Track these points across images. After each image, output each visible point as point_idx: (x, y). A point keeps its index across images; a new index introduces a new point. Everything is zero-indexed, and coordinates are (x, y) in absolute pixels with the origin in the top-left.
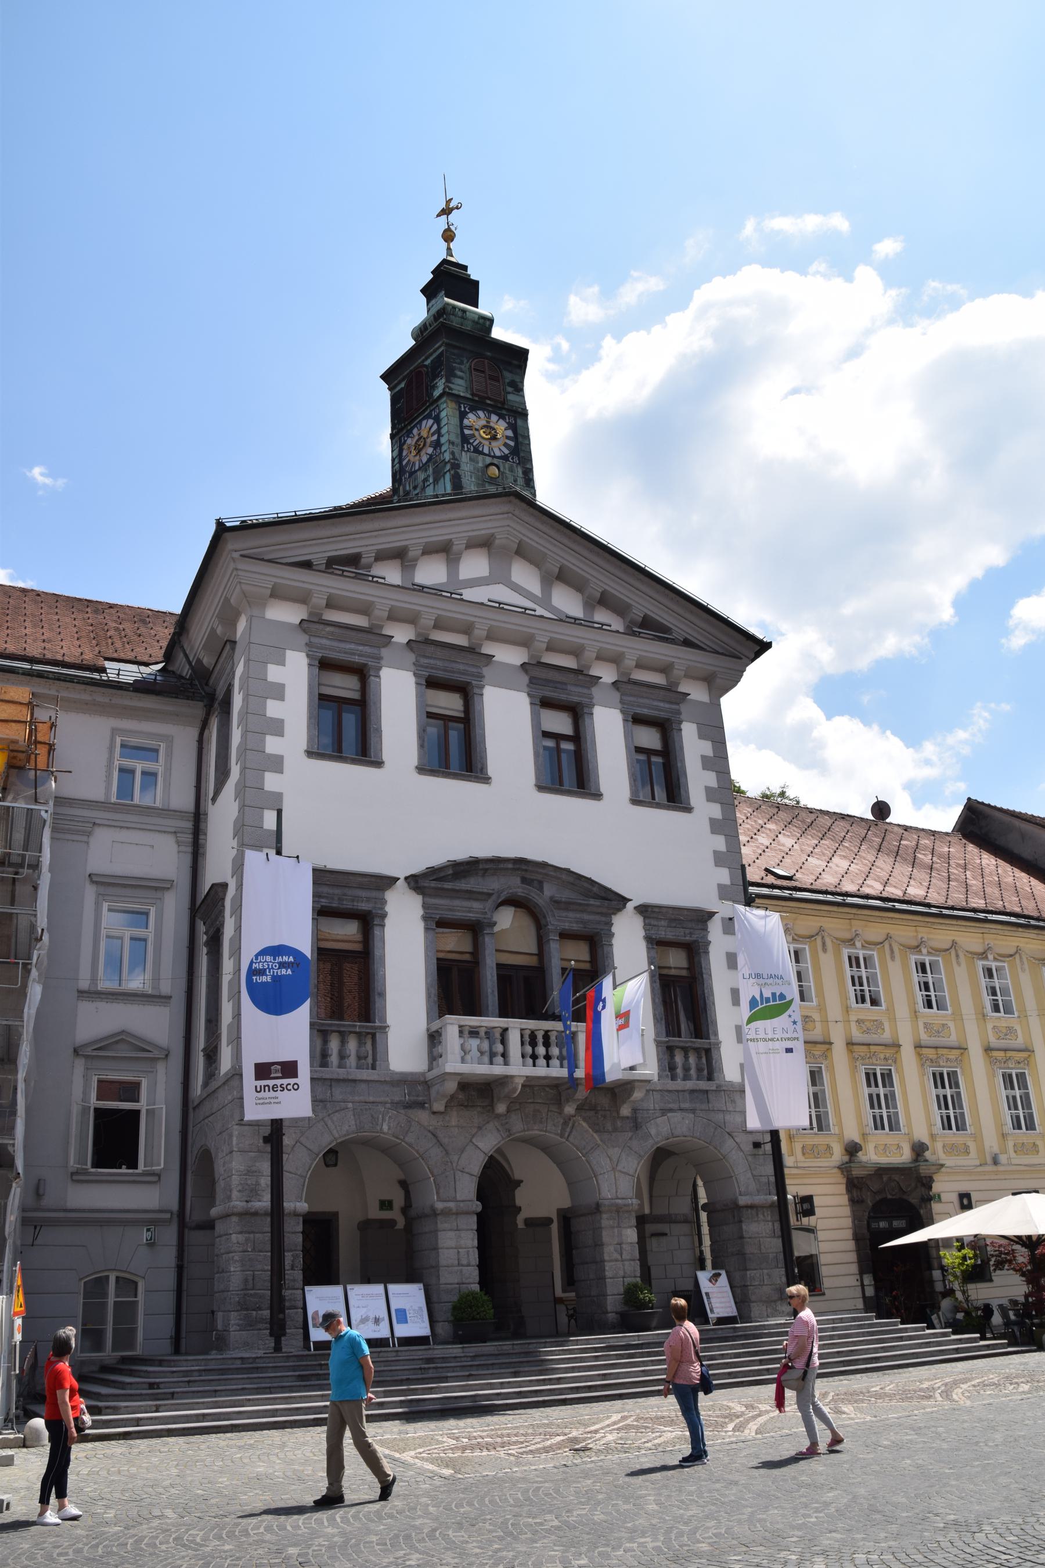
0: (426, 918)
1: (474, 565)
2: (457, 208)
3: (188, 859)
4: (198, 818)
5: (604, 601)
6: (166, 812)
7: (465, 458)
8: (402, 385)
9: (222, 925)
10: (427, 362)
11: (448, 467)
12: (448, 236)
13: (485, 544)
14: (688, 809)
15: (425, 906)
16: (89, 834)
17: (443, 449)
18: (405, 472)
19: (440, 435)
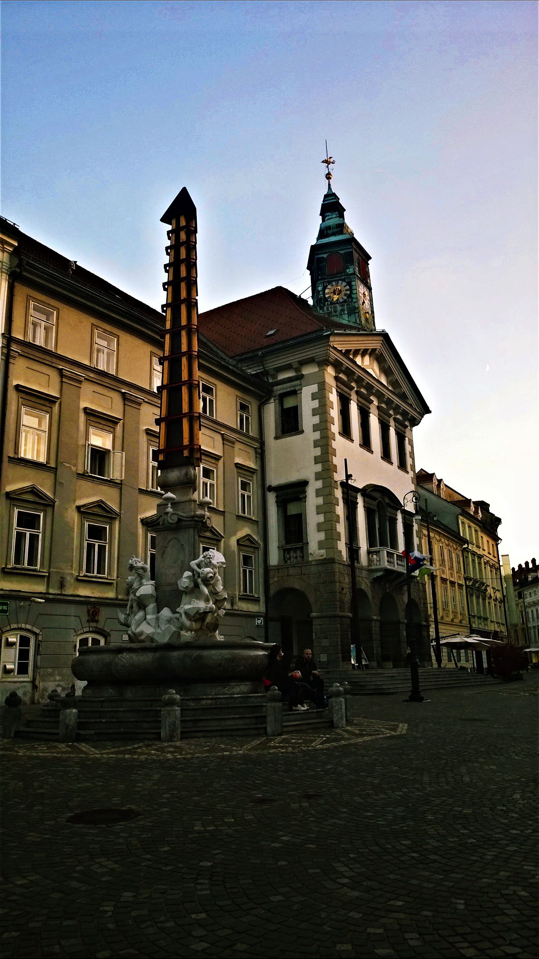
0: (364, 507)
1: (367, 358)
2: (333, 163)
3: (259, 460)
4: (262, 443)
5: (394, 384)
8: (325, 256)
9: (306, 497)
10: (342, 252)
12: (328, 176)
14: (408, 472)
15: (364, 502)
17: (354, 300)
19: (351, 293)
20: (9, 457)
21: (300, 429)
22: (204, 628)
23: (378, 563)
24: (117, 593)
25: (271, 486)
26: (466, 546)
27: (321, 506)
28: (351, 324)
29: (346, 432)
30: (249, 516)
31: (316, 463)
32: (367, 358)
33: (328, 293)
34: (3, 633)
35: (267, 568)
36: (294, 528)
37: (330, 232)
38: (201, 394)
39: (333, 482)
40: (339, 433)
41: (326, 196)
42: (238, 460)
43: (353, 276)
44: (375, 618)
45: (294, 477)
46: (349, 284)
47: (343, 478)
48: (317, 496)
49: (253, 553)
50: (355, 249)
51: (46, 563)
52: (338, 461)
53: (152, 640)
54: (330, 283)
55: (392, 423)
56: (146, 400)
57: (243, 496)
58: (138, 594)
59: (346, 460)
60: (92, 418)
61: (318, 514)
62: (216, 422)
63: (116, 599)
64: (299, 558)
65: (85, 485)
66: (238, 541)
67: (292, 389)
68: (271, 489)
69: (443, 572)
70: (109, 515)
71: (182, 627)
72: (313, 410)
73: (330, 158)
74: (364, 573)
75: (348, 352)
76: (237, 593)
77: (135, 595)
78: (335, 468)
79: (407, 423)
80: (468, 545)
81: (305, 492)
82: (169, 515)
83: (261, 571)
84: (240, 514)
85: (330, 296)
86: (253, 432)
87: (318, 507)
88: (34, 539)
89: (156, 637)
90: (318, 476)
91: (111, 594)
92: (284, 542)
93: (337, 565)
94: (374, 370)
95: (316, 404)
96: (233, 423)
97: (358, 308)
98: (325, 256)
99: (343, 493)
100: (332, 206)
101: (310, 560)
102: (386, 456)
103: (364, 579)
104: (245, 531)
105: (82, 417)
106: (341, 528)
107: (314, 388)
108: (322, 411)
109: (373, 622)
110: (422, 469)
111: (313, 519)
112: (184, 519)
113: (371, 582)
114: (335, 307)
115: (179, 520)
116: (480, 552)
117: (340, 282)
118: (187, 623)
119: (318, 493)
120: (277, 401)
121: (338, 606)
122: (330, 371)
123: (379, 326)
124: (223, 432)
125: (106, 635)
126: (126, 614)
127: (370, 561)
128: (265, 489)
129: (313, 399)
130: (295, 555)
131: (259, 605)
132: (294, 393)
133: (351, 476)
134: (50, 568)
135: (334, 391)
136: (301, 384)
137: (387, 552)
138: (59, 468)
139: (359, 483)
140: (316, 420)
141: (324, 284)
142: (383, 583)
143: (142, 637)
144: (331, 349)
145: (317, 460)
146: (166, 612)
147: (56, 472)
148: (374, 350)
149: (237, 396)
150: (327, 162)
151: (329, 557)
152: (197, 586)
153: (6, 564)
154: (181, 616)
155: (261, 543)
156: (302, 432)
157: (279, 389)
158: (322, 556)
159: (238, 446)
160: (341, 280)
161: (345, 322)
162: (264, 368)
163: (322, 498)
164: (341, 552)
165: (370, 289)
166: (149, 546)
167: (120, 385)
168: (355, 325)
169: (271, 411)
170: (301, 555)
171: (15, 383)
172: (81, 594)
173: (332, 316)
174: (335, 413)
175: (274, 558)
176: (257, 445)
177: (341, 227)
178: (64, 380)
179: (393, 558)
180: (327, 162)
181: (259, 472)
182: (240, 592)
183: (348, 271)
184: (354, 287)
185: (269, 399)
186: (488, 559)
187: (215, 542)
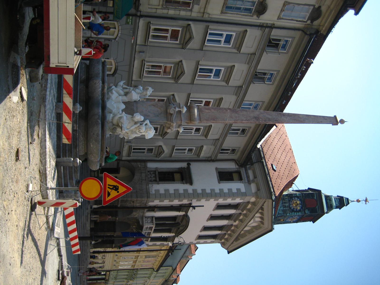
0: (177, 216)
2: (366, 203)
3: (204, 159)
4: (213, 161)
6: (216, 156)
7: (287, 217)
8: (315, 198)
9: (184, 184)
10: (317, 207)
11: (285, 215)
12: (358, 201)
13: (262, 223)
14: (196, 240)
15: (180, 216)
16: (214, 145)
17: (291, 213)
18: (291, 199)
19: (295, 212)
20: (209, 26)
21: (221, 182)
22: (114, 126)
23: (146, 222)
24: (135, 81)
25: (190, 165)
26: (155, 270)
27: (178, 192)
28: (278, 211)
29: (219, 207)
30: (174, 152)
31: (202, 190)
32: (259, 219)
33: (295, 199)
34: (117, 22)
35: (145, 161)
36: (166, 177)
37: (328, 201)
38: (241, 128)
39: (191, 199)
40: (218, 203)
41: (348, 199)
42: (205, 148)
43: (304, 213)
44: (117, 219)
45: (195, 177)
46: (300, 211)
47: (193, 204)
48: (184, 190)
49: (154, 154)
50: (318, 214)
51: (152, 44)
52: (203, 202)
53: (108, 99)
54: (300, 200)
55: (223, 232)
56: (238, 98)
57: (185, 150)
58: (133, 92)
59: (203, 206)
60: (229, 69)
61: (174, 190)
62: (226, 136)
63: (132, 80)
64: (150, 179)
65: (193, 65)
66: (161, 146)
67: (243, 178)
68: (189, 165)
69: (141, 257)
70: (177, 78)
71: (115, 115)
72: (231, 189)
73: (369, 202)
74: (141, 214)
75: (262, 208)
76: (132, 145)
77: (132, 90)
78: (199, 200)
79: (223, 241)
80: (156, 271)
81: (186, 183)
82: (174, 109)
83: (144, 158)
84: (175, 148)
85: (293, 200)
86: (220, 156)
87: (178, 190)
88: (165, 38)
89: (110, 100)
90: (195, 191)
91: (134, 78)
92: (160, 171)
93: (146, 200)
94: (253, 224)
95: (234, 191)
96: (225, 146)
97: (286, 215)
98: (315, 198)
99: (185, 204)
100: (342, 202)
101: (150, 185)
102: (206, 228)
103: (138, 214)
104: (166, 150)
105: (231, 64)
106: (166, 203)
107: (243, 190)
108: (231, 194)
109: (115, 218)
110: (198, 248)
111: (171, 187)
112: (172, 118)
113: (136, 217)
114: (287, 203)
115: (171, 115)
116: (152, 278)
117: (301, 206)
118: (116, 118)
119: (186, 191)
120: (237, 170)
121: (124, 199)
122: (253, 199)
123: (275, 226)
124: (220, 139)
125: (113, 74)
126: (123, 85)
127: (149, 217)
128: (189, 162)
129: (237, 189)
130: (152, 177)
131: (126, 157)
132: (240, 179)
133: (194, 209)
134: (150, 46)
135: (241, 201)
136: (245, 183)
137: (152, 227)
138: (203, 51)
139: (191, 213)
140: (226, 191)
141: (300, 197)
142: (136, 224)
143: (110, 93)
144: (264, 200)
145: (203, 190)
146: (123, 106)
147: (200, 50)
148: (262, 223)
149: (240, 147)
150: (366, 200)
151: (150, 195)
152: (136, 123)
153: (152, 24)
154: (120, 114)
155: (159, 159)
156: (219, 183)
157: (243, 171)
158: (151, 191)
159: (213, 148)
160: (302, 206)
161: (279, 208)
162: (255, 163)
163: (183, 192)
164: (153, 202)
165: (297, 222)
166: (159, 98)
167: (246, 85)
168: (277, 214)
169: (231, 166)
170: (152, 180)
171: (248, 30)
172: (135, 62)
173: (282, 201)
174: (229, 201)
175: (151, 165)
176: (213, 159)
177: (330, 208)
178: (249, 55)
179: (149, 230)
180: (366, 200)
181: (198, 159)
182: (134, 146)
183: (307, 210)
184: (298, 214)
185: (238, 165)
186: (148, 282)
187: (161, 133)
